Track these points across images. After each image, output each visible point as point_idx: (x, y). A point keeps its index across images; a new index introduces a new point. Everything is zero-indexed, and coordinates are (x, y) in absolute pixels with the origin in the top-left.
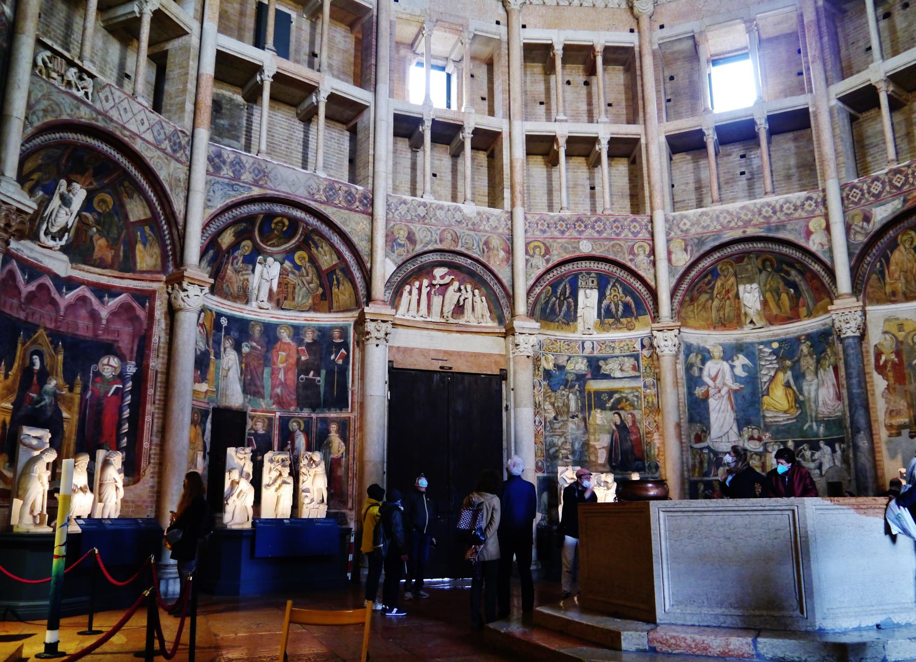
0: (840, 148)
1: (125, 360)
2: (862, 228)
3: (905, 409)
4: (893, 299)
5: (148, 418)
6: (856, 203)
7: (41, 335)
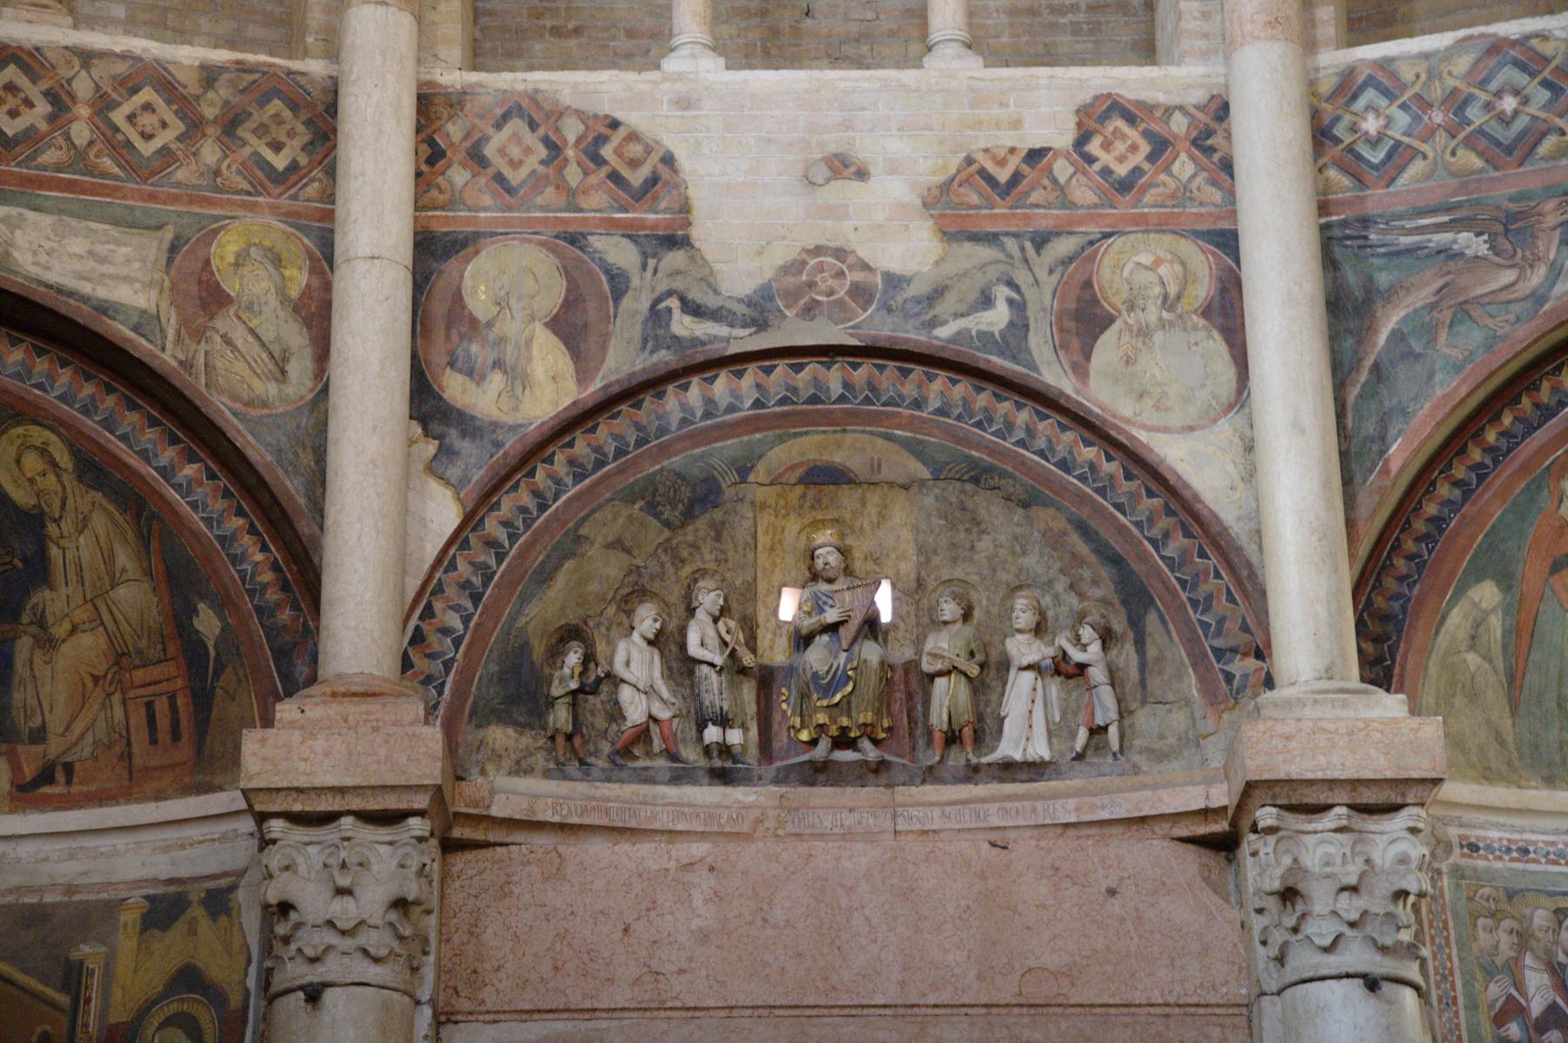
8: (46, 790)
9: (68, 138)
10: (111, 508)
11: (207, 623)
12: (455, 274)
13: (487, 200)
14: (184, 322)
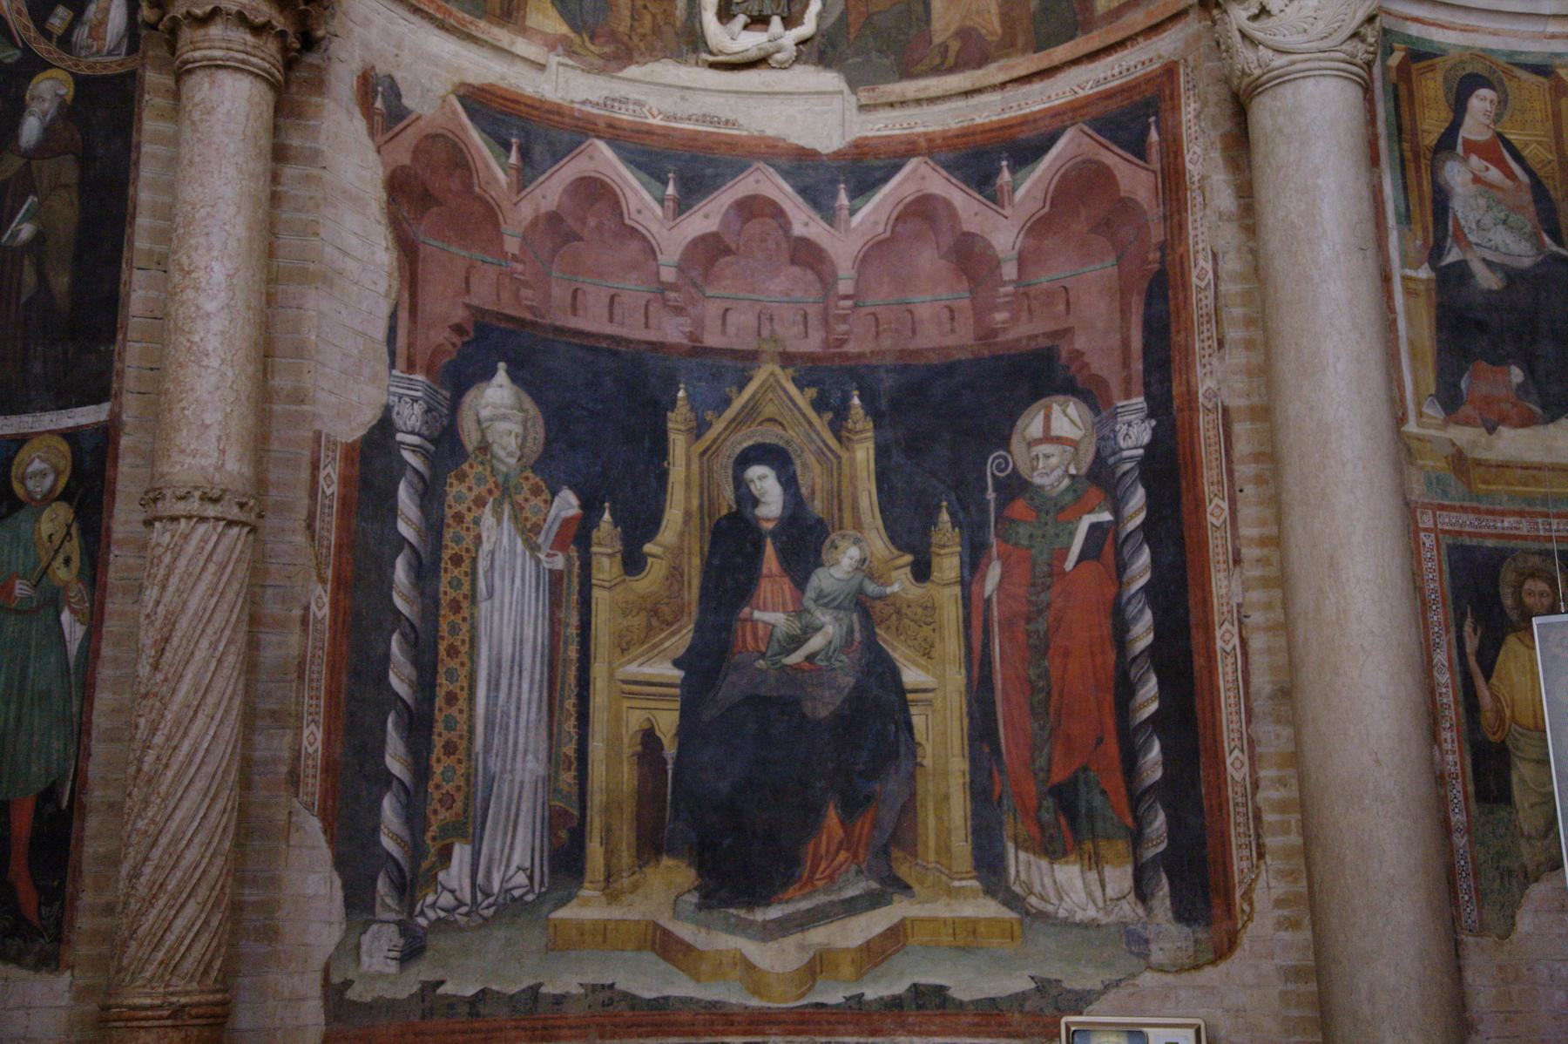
1: (1109, 403)
5: (1225, 638)
7: (771, 386)
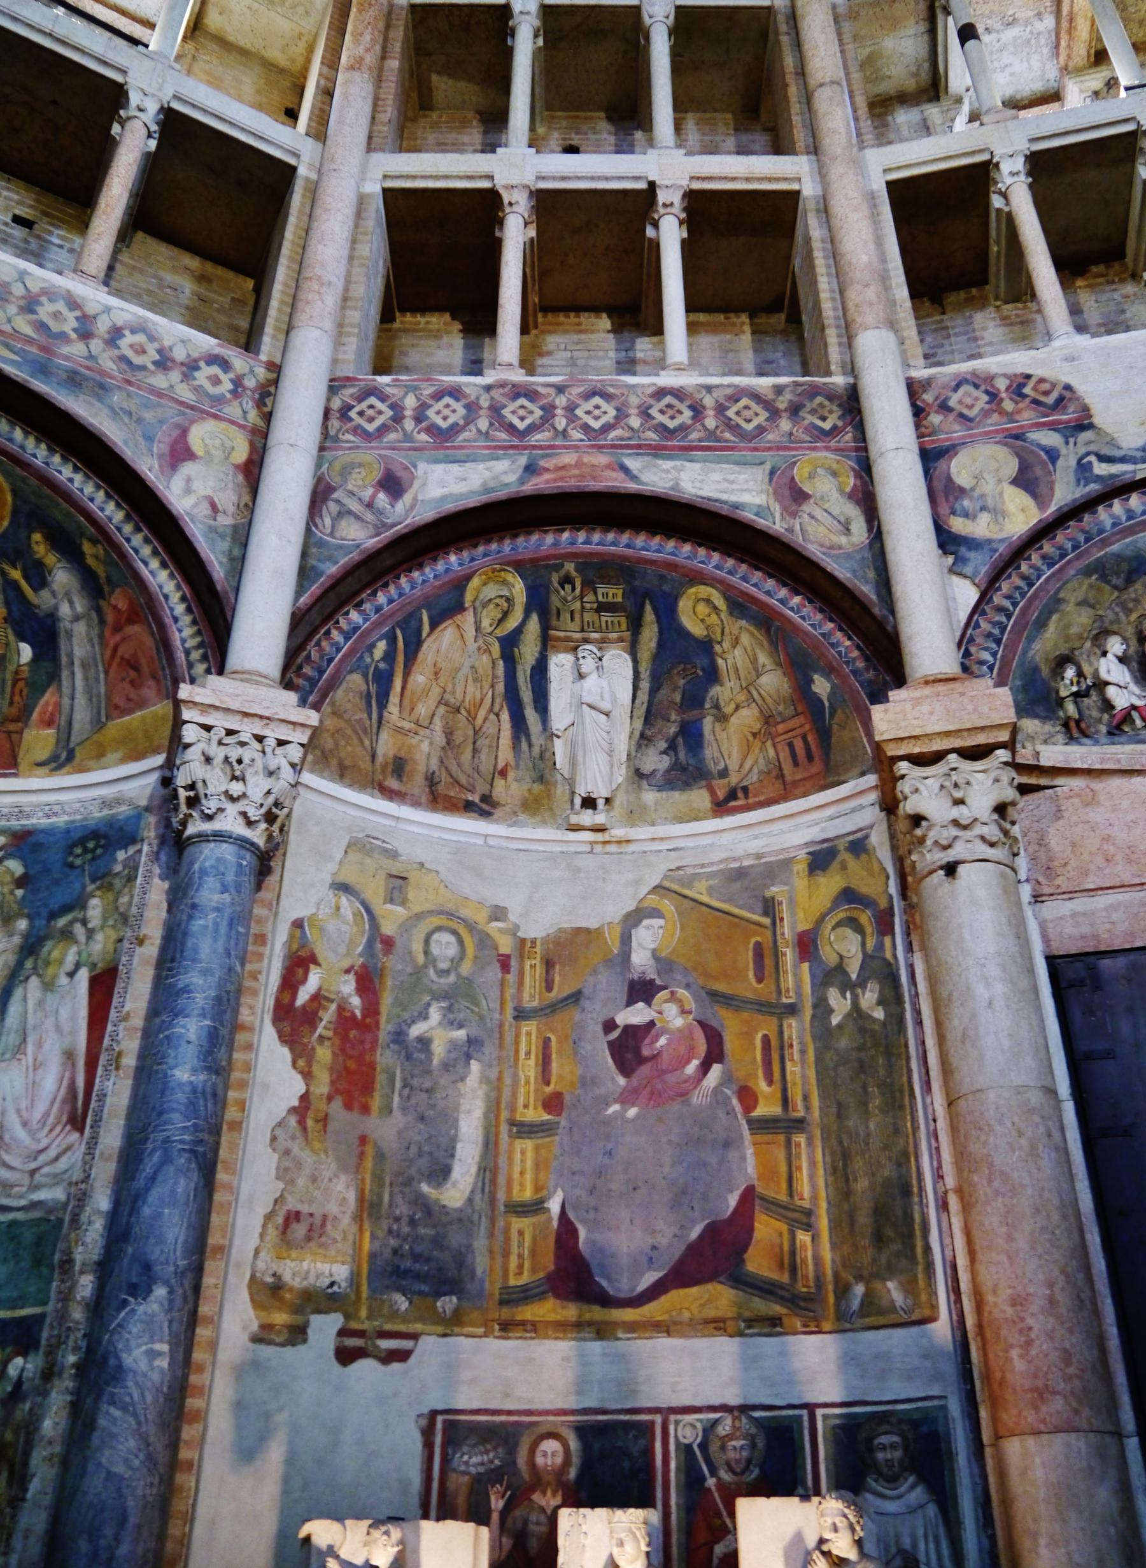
0: (359, 290)
2: (370, 505)
3: (346, 1221)
4: (392, 783)
6: (367, 436)
8: (733, 803)
9: (704, 426)
10: (752, 628)
11: (821, 686)
12: (945, 467)
13: (957, 427)
14: (785, 509)
